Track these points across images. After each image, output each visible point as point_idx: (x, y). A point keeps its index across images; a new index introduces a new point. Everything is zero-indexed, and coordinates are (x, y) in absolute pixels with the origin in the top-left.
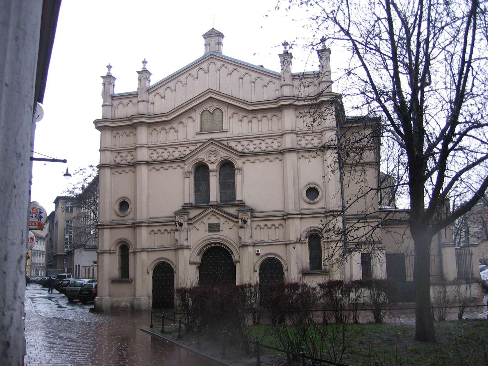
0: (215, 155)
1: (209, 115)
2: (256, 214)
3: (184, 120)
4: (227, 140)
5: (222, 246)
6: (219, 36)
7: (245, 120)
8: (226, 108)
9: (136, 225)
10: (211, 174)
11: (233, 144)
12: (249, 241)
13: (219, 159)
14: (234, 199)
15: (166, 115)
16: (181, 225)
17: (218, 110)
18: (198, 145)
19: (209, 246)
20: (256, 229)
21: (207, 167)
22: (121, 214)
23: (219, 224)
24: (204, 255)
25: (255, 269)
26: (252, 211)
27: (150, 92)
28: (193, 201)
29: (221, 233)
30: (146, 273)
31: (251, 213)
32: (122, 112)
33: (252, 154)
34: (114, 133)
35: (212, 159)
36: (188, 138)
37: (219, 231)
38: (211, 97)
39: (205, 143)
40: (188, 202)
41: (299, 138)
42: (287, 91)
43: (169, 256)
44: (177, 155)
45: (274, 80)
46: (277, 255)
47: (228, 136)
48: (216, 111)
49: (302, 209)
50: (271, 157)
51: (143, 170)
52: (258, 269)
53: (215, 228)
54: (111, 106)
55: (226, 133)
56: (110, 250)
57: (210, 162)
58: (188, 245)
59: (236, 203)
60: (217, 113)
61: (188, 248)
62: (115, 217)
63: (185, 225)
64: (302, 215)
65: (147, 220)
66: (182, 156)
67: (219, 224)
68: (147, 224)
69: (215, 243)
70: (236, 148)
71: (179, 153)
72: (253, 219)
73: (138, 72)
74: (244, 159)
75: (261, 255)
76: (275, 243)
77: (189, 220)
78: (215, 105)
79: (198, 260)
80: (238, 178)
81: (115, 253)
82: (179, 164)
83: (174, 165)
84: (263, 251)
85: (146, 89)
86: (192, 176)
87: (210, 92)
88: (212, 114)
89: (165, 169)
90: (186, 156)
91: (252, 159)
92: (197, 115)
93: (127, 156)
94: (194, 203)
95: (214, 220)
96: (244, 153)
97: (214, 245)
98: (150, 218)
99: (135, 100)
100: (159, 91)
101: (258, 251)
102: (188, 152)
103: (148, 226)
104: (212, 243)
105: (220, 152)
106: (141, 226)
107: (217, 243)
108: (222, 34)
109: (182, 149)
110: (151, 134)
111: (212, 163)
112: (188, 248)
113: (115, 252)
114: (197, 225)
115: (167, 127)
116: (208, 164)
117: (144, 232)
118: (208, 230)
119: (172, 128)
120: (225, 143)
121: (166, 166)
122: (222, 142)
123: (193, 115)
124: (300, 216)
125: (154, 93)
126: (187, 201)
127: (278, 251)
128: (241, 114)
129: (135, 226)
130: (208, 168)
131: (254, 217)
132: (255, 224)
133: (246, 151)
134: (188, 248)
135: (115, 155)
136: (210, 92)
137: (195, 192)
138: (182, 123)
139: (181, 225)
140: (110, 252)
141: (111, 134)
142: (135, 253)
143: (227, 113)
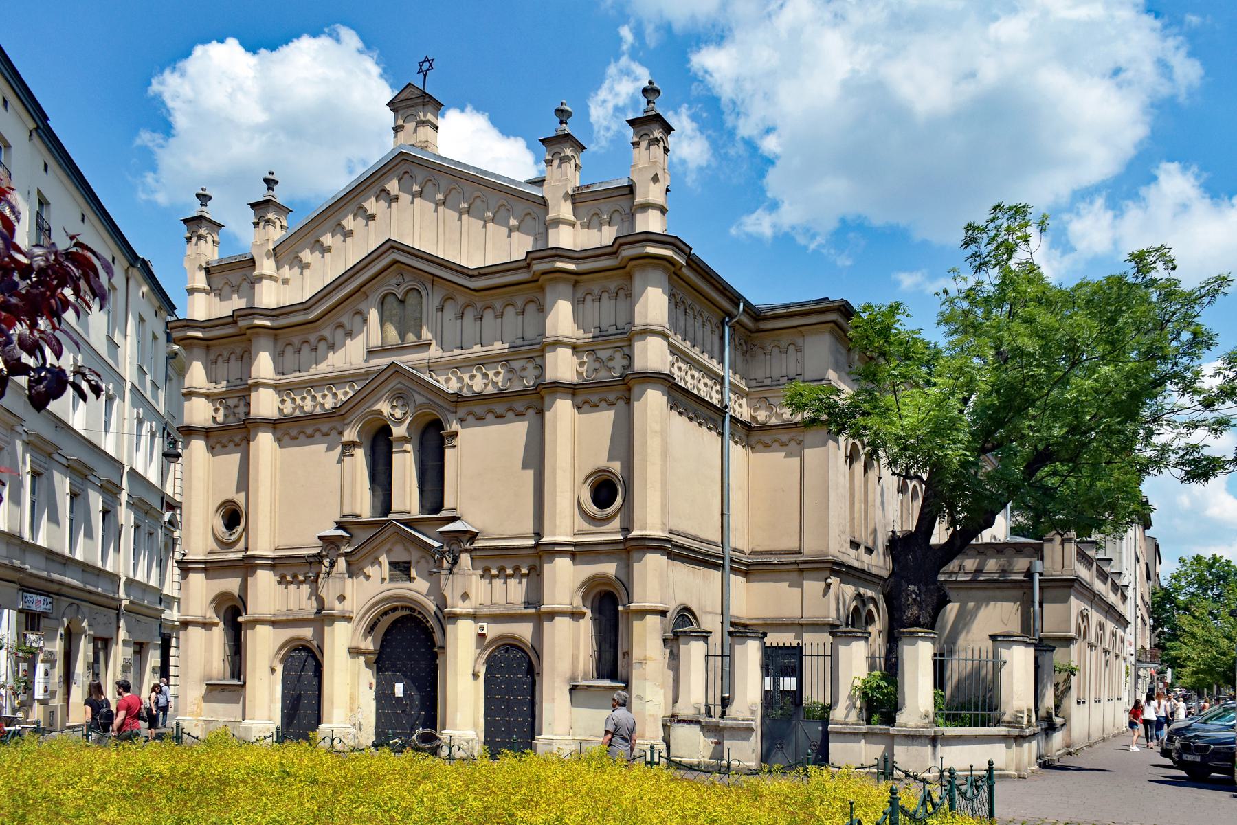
1: (395, 304)
7: (470, 315)
8: (429, 286)
12: (460, 608)
14: (439, 507)
15: (305, 306)
17: (415, 293)
23: (409, 562)
24: (388, 632)
26: (473, 536)
30: (268, 670)
35: (398, 413)
38: (396, 262)
42: (564, 238)
44: (329, 403)
46: (520, 641)
48: (410, 295)
50: (519, 405)
59: (442, 514)
60: (412, 299)
64: (575, 545)
67: (409, 562)
69: (403, 608)
73: (253, 206)
75: (488, 639)
82: (334, 424)
84: (492, 630)
85: (271, 247)
86: (360, 453)
88: (402, 302)
91: (479, 410)
93: (236, 407)
95: (401, 555)
101: (482, 628)
104: (394, 609)
105: (416, 395)
107: (407, 608)
110: (282, 354)
111: (399, 422)
115: (313, 338)
117: (264, 580)
118: (387, 577)
119: (323, 339)
123: (362, 306)
124: (572, 549)
127: (524, 631)
128: (461, 300)
129: (248, 566)
130: (391, 433)
133: (465, 392)
138: (341, 326)
141: (207, 355)
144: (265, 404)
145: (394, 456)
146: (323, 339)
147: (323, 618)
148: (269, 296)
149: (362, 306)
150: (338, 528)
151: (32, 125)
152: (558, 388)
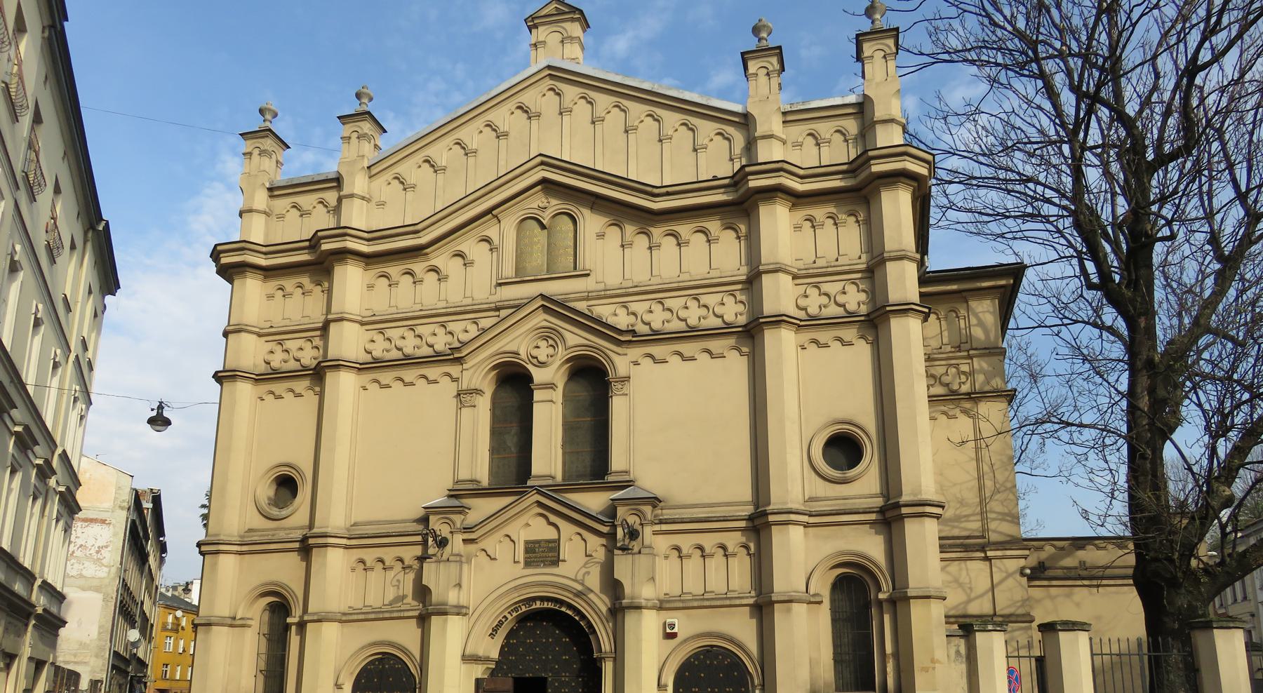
0: (551, 342)
2: (667, 514)
3: (469, 244)
4: (587, 299)
5: (563, 609)
6: (573, 20)
8: (586, 212)
9: (311, 541)
10: (538, 395)
11: (604, 311)
12: (647, 593)
13: (562, 354)
16: (442, 543)
17: (566, 218)
18: (504, 313)
19: (524, 609)
20: (666, 557)
21: (528, 378)
22: (275, 512)
25: (663, 682)
26: (654, 501)
27: (374, 171)
28: (483, 475)
29: (562, 569)
31: (654, 507)
32: (296, 229)
33: (657, 337)
34: (273, 284)
35: (542, 354)
36: (475, 297)
37: (556, 562)
38: (544, 181)
39: (518, 307)
40: (469, 477)
41: (801, 289)
43: (405, 635)
44: (441, 342)
45: (730, 130)
46: (731, 640)
47: (590, 289)
49: (811, 499)
50: (716, 345)
51: (343, 385)
52: (669, 680)
53: (542, 554)
54: (265, 213)
55: (584, 279)
56: (234, 618)
57: (535, 361)
58: (463, 602)
59: (610, 478)
61: (458, 614)
62: (259, 522)
63: (457, 543)
65: (348, 530)
66: (457, 345)
67: (558, 541)
68: (344, 541)
69: (543, 599)
70: (611, 321)
71: (449, 338)
72: (657, 528)
74: (635, 352)
76: (728, 602)
77: (467, 529)
78: (555, 204)
79: (492, 649)
80: (618, 406)
81: (249, 626)
83: (433, 372)
85: (366, 165)
86: (484, 405)
87: (542, 163)
89: (406, 384)
90: (464, 344)
91: (657, 350)
92: (505, 230)
94: (485, 482)
95: (540, 530)
96: (633, 332)
97: (538, 605)
98: (355, 524)
99: (331, 197)
100: (399, 169)
101: (672, 626)
102: (473, 330)
103: (347, 547)
106: (326, 546)
108: (581, 12)
109: (456, 327)
110: (371, 287)
111: (542, 364)
112: (460, 611)
113: (249, 622)
114: (490, 544)
115: (418, 267)
116: (530, 367)
118: (522, 560)
120: (581, 306)
121: (409, 374)
122: (571, 305)
125: (389, 175)
126: (464, 474)
131: (661, 522)
132: (662, 544)
133: (641, 328)
134: (460, 611)
135: (272, 346)
136: (542, 163)
137: (493, 451)
139: (442, 543)
140: (234, 623)
142: (302, 626)
143: (591, 222)
144: (349, 342)
145: (537, 408)
146: (435, 270)
147: (427, 610)
148: (357, 216)
149: (492, 232)
150: (450, 496)
151: (46, 23)
152: (779, 321)
